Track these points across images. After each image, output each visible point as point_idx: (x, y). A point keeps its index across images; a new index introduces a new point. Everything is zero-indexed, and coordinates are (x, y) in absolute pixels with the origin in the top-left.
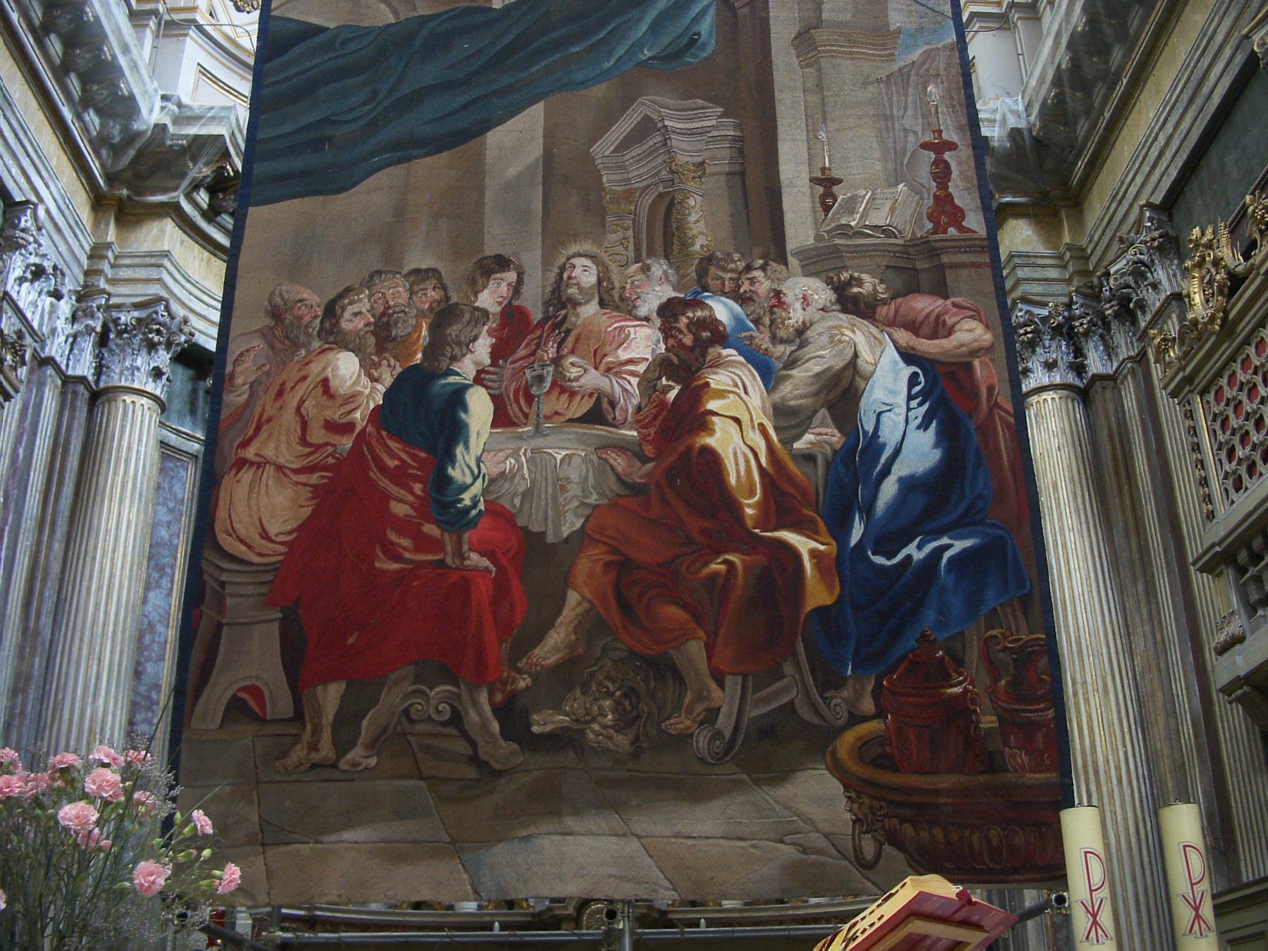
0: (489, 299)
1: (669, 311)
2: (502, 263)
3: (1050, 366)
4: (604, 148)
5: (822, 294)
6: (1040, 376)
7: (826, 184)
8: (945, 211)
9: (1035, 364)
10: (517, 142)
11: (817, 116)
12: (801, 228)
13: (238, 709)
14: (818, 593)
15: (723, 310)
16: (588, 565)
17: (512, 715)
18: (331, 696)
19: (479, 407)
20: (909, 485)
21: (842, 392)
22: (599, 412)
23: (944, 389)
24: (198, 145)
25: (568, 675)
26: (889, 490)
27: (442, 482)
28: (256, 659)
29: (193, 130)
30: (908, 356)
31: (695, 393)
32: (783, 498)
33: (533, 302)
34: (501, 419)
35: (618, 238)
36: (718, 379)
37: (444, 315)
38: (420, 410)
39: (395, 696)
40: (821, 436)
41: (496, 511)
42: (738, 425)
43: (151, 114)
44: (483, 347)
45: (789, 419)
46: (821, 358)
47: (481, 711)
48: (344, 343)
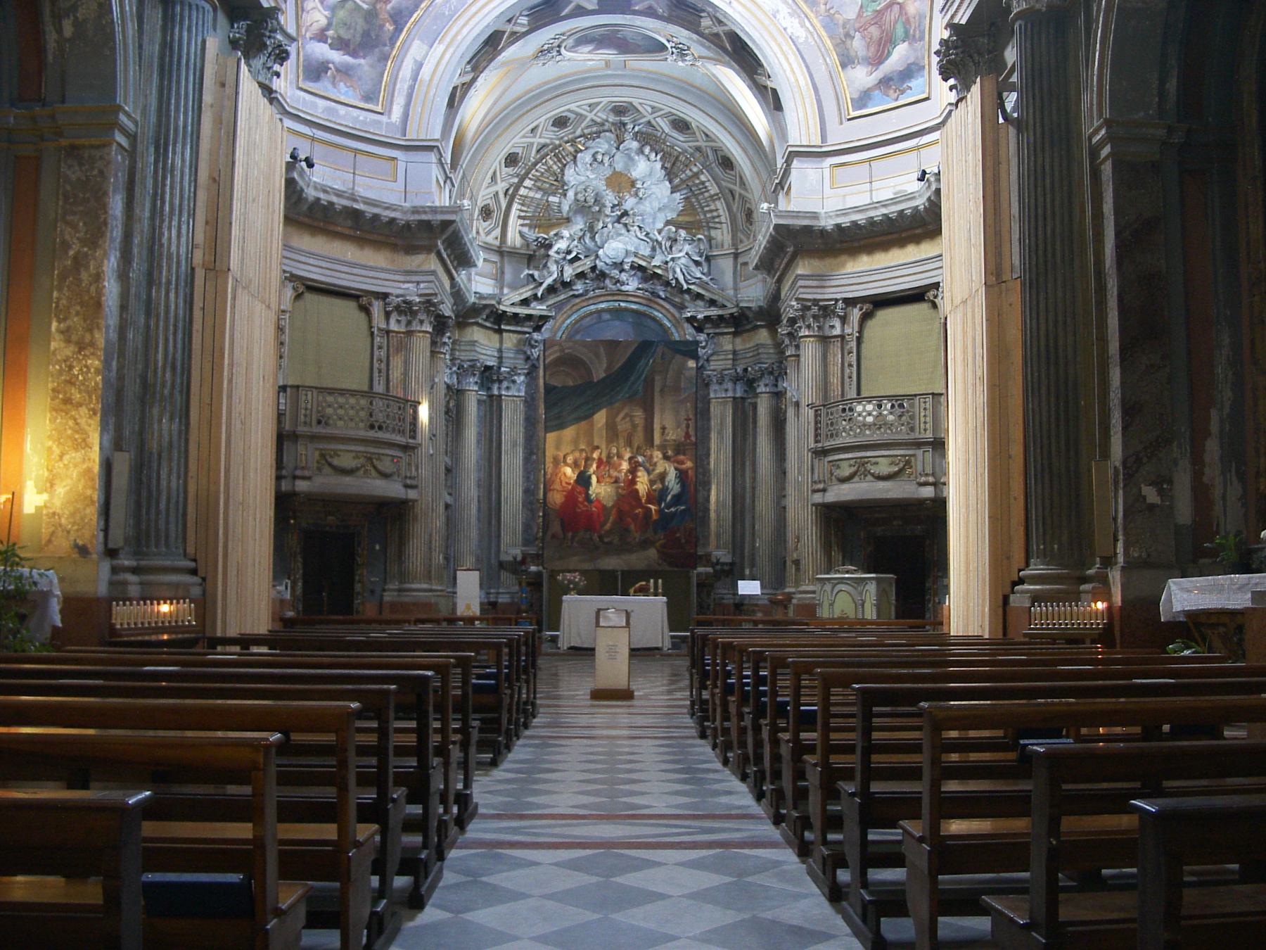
0: (595, 455)
1: (630, 459)
2: (597, 448)
3: (766, 385)
4: (618, 419)
5: (660, 456)
6: (761, 389)
7: (663, 428)
8: (687, 435)
9: (761, 383)
10: (601, 418)
11: (662, 411)
12: (657, 441)
13: (554, 536)
14: (655, 517)
15: (640, 459)
16: (614, 512)
17: (601, 537)
18: (570, 534)
19: (594, 479)
20: (674, 496)
21: (662, 477)
22: (616, 481)
23: (682, 476)
24: (486, 306)
25: (609, 533)
26: (669, 497)
27: (588, 496)
28: (556, 527)
29: (484, 302)
30: (676, 469)
31: (635, 477)
32: (649, 500)
33: (604, 457)
34: (598, 481)
35: (621, 442)
36: (639, 474)
37: (587, 459)
38: (583, 480)
39: (581, 533)
40: (658, 486)
41: (598, 501)
42: (642, 485)
43: (472, 299)
44: (595, 466)
45: (652, 482)
46: (659, 470)
47: (595, 536)
48: (568, 465)
